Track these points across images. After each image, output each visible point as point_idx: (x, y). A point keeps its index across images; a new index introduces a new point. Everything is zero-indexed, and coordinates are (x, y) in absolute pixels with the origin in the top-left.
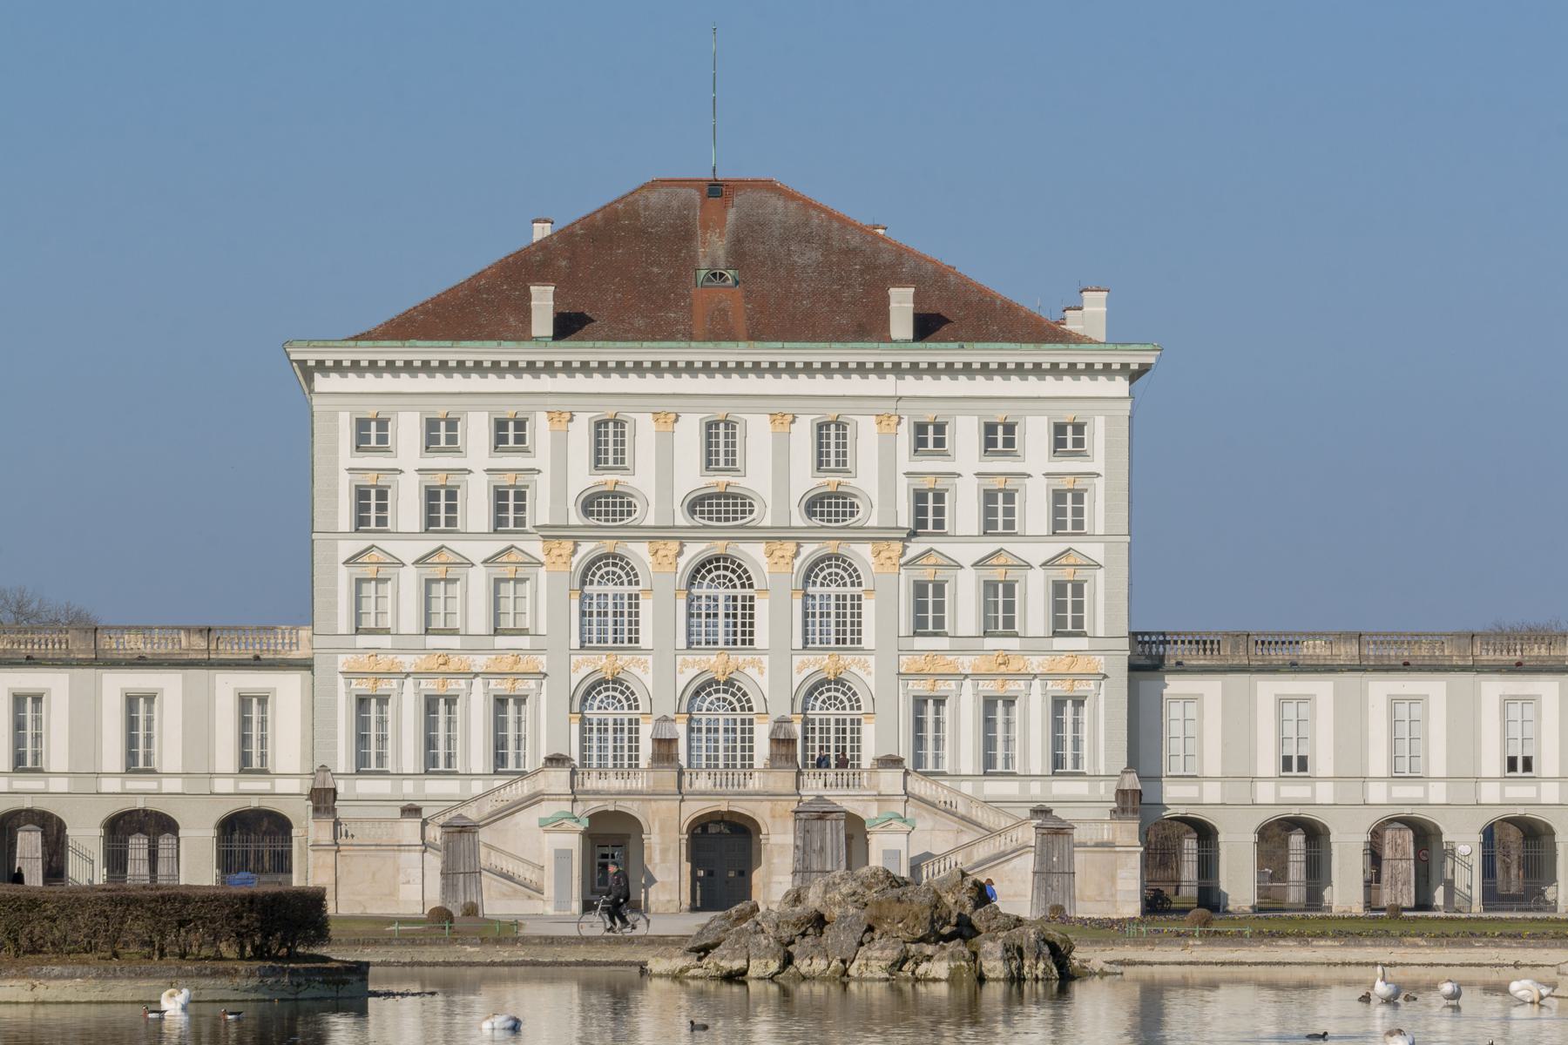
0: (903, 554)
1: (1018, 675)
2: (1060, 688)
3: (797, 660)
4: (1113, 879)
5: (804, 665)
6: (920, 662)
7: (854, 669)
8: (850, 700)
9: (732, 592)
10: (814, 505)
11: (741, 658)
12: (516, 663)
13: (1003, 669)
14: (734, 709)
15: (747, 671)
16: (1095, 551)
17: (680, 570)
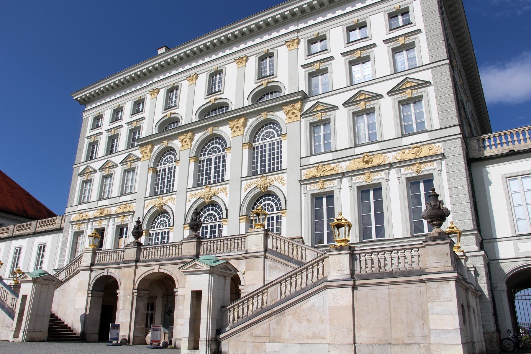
0: (301, 109)
1: (379, 167)
2: (410, 172)
3: (244, 183)
4: (424, 316)
5: (248, 186)
6: (314, 172)
7: (276, 183)
8: (276, 204)
9: (218, 154)
10: (258, 96)
11: (217, 188)
12: (125, 208)
13: (369, 165)
14: (216, 219)
15: (219, 195)
16: (426, 75)
17: (192, 148)
